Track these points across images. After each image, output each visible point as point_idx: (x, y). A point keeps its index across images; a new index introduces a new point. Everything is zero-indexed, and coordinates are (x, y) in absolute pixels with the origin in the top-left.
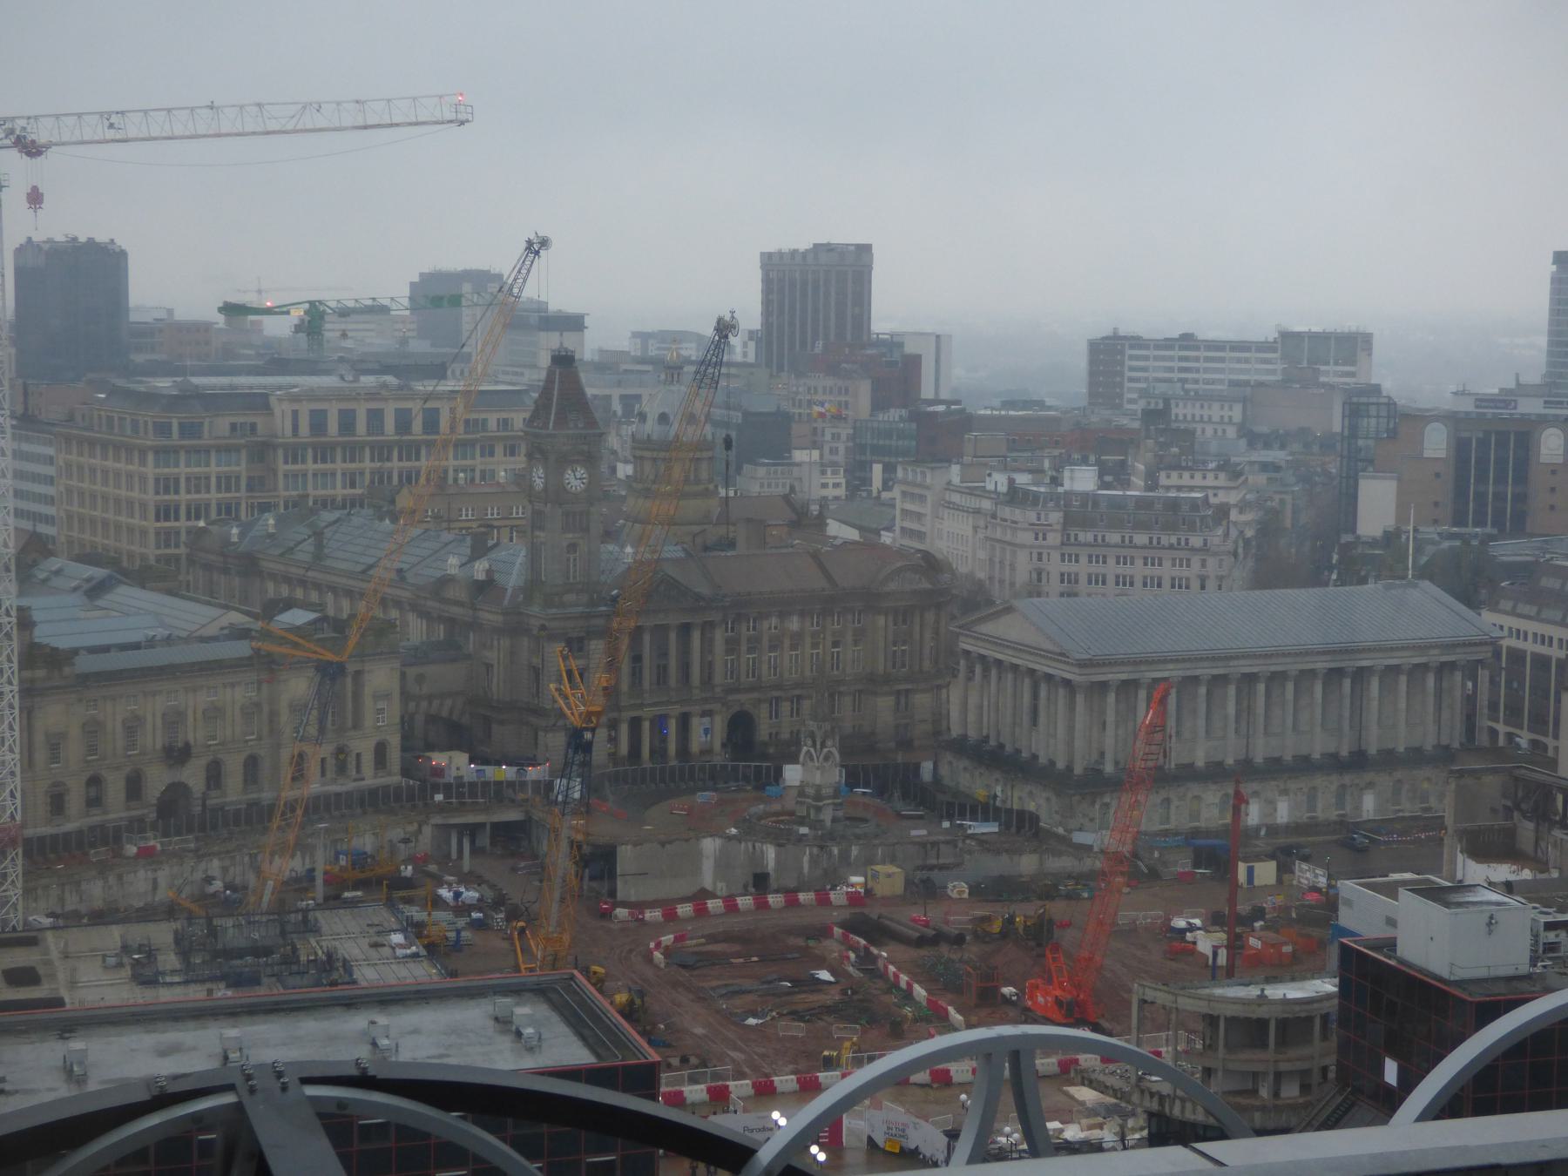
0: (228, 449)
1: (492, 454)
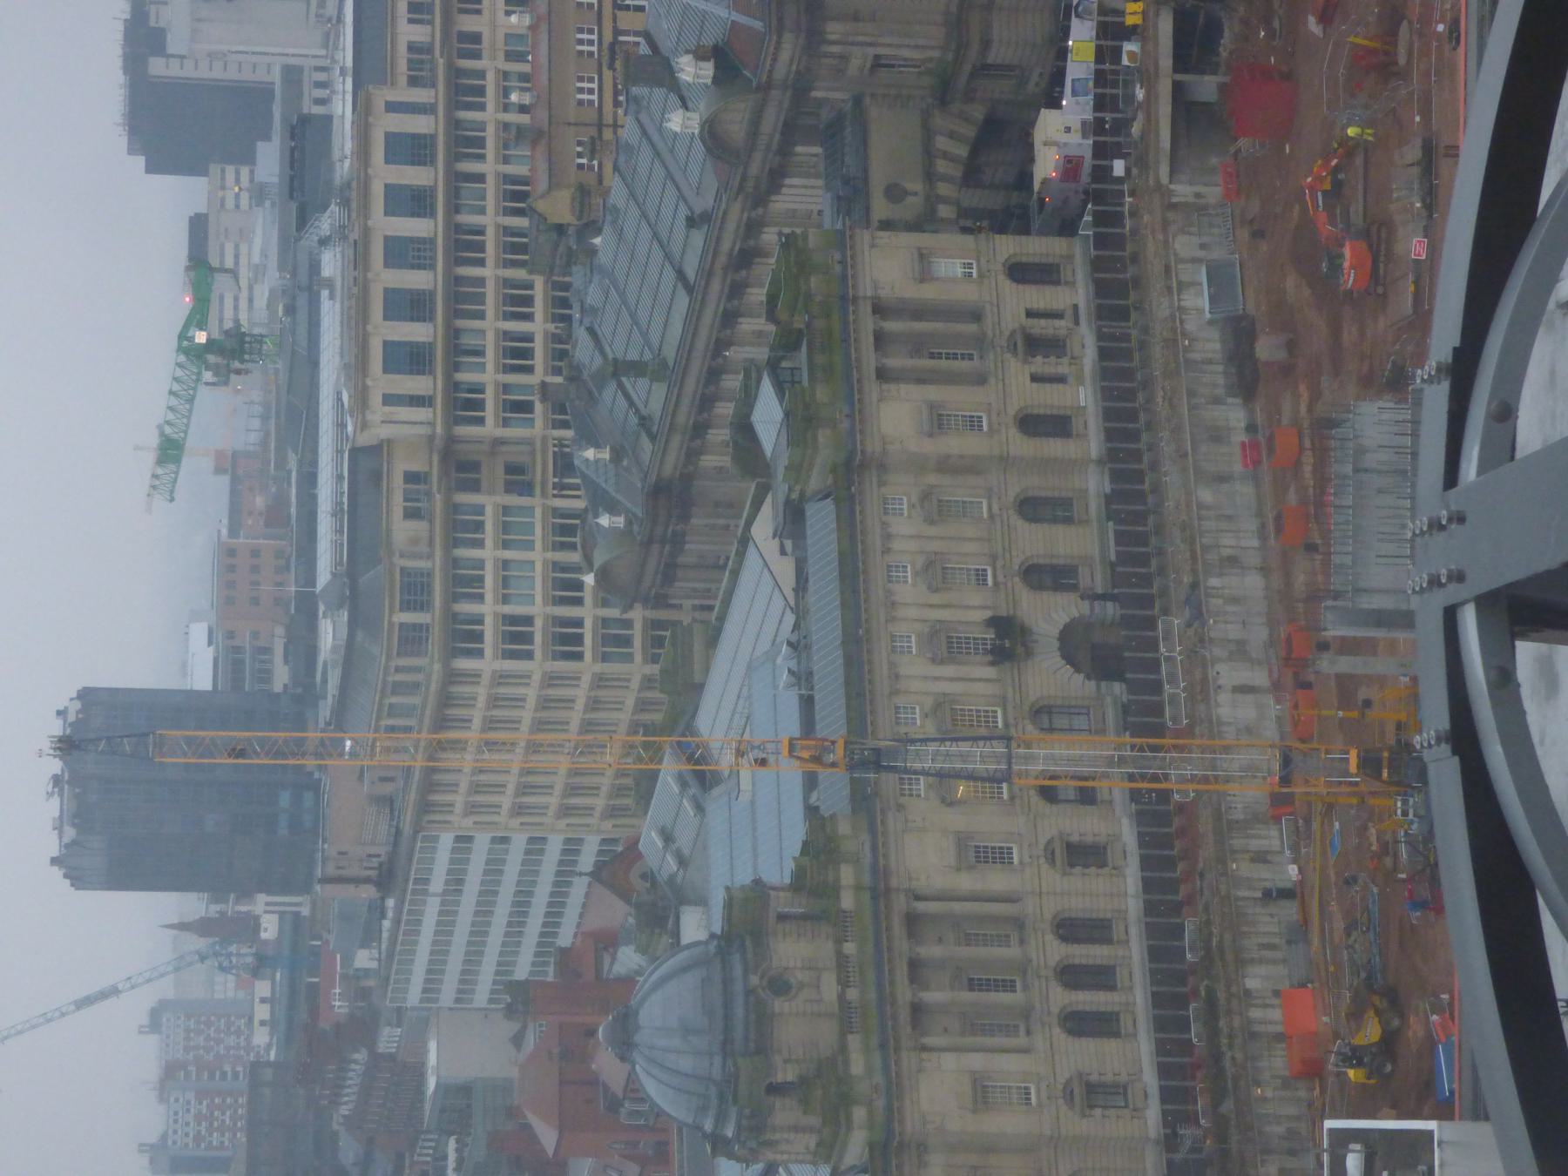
1: (476, 38)
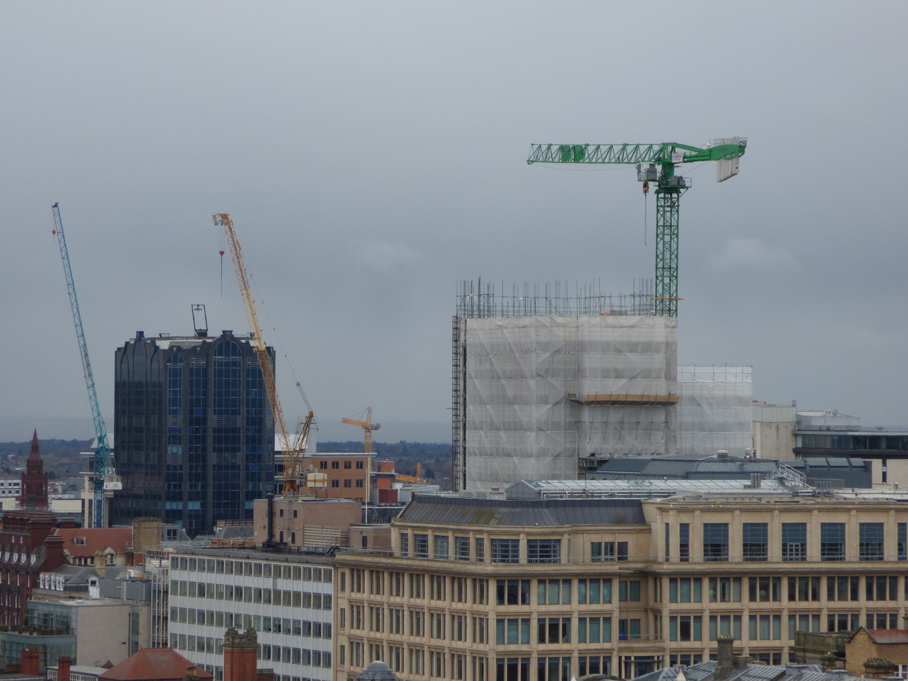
0: (595, 579)
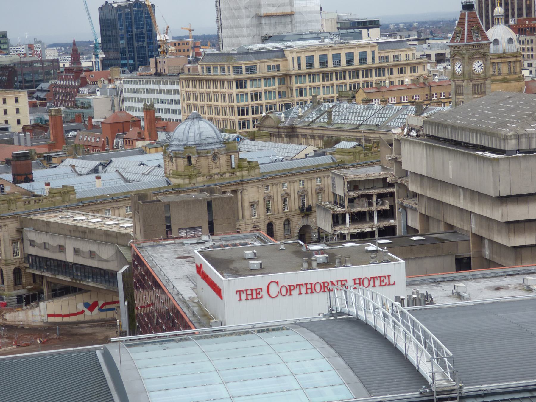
0: (269, 78)
1: (392, 73)
